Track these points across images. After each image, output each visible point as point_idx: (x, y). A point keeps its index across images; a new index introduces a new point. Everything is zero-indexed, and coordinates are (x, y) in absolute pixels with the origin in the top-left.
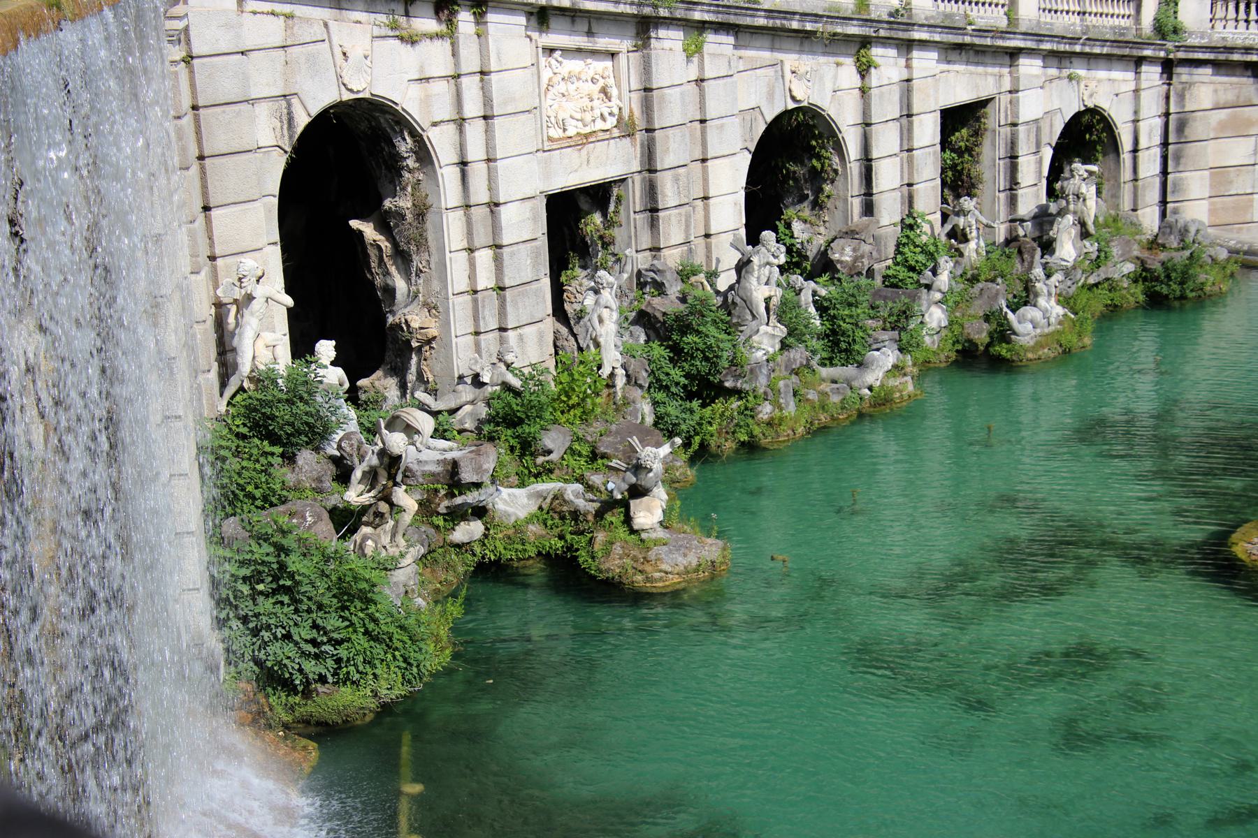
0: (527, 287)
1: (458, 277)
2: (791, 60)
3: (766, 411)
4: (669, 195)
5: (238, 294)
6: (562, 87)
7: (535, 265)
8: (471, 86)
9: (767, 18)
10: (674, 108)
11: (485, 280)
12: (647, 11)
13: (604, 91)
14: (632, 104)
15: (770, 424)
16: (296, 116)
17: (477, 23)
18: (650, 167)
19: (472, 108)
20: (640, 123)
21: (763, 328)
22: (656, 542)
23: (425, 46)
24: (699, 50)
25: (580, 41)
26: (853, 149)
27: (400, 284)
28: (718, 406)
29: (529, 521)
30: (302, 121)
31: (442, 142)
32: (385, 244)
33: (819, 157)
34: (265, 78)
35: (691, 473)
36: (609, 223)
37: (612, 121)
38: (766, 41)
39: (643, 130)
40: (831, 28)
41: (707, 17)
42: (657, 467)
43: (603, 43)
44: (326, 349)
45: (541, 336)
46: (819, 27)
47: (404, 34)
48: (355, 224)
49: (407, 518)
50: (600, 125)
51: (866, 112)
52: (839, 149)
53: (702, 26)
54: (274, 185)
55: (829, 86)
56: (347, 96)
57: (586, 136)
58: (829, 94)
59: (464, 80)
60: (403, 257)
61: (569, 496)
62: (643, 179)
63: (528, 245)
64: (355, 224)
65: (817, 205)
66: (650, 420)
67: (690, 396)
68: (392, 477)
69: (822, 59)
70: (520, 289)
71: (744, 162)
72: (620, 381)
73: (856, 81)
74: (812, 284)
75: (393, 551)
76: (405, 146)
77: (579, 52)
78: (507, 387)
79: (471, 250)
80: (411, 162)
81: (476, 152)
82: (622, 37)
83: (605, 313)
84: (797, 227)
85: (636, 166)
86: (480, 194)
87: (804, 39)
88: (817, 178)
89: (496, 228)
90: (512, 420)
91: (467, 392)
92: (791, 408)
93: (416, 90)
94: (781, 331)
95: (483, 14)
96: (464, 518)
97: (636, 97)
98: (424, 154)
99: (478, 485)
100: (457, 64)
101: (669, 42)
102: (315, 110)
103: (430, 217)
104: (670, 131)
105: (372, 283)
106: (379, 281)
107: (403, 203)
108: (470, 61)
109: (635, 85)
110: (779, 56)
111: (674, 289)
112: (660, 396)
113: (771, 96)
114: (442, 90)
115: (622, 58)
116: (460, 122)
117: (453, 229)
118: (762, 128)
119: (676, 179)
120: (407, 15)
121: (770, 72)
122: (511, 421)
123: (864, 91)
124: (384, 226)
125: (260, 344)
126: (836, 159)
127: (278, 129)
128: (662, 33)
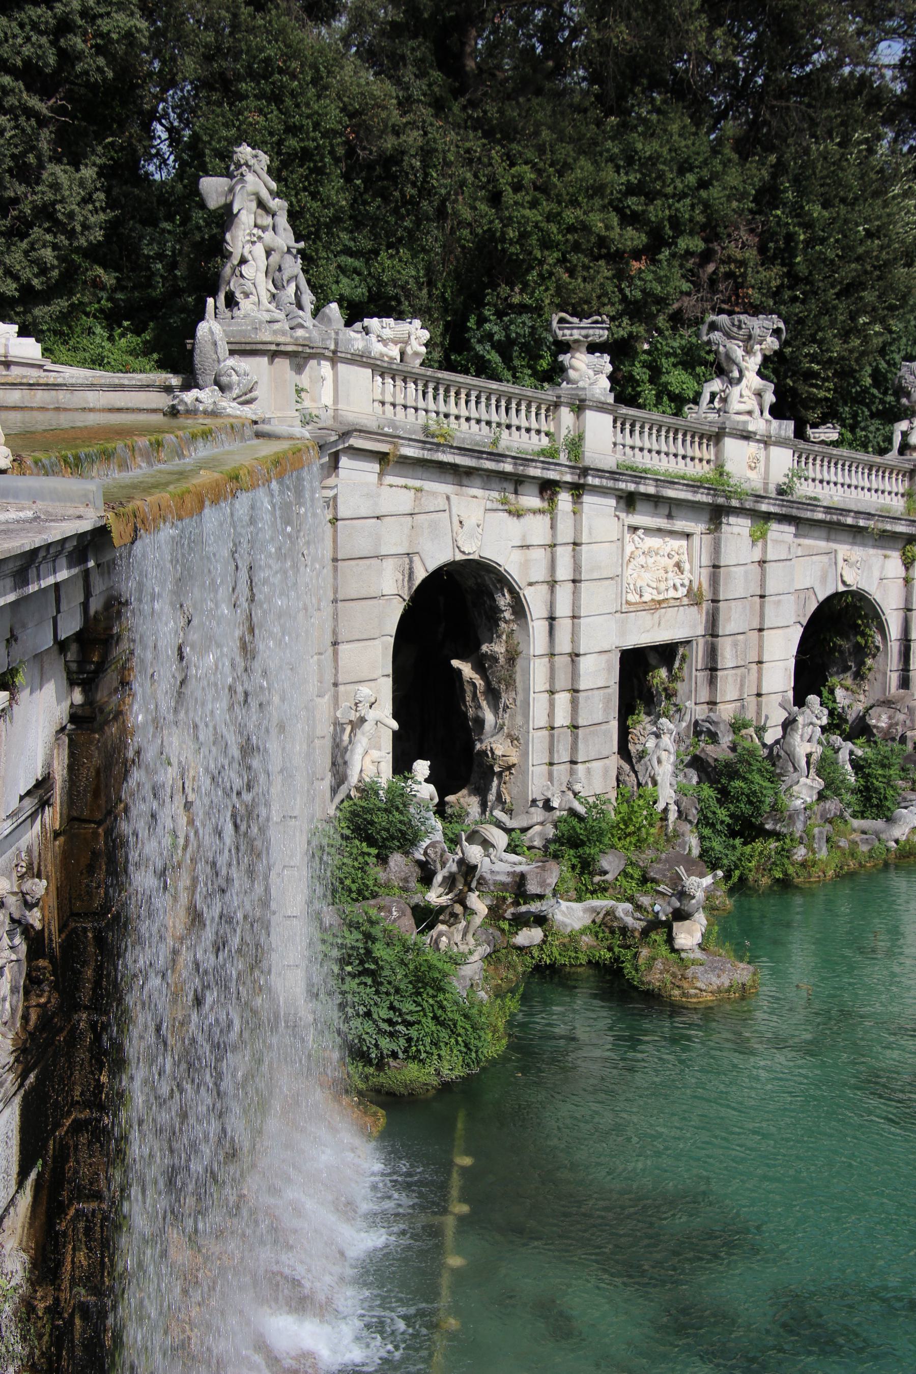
1: (538, 714)
2: (843, 550)
3: (800, 853)
4: (727, 657)
5: (353, 716)
6: (642, 560)
7: (606, 709)
8: (564, 555)
10: (738, 584)
11: (562, 718)
12: (721, 501)
13: (678, 565)
14: (702, 578)
15: (804, 865)
17: (574, 503)
19: (564, 572)
20: (707, 594)
21: (803, 780)
22: (694, 962)
23: (529, 519)
24: (763, 536)
25: (660, 522)
26: (894, 631)
27: (489, 717)
28: (758, 845)
29: (583, 932)
30: (420, 575)
31: (535, 600)
32: (479, 683)
33: (863, 635)
34: (394, 539)
35: (729, 903)
36: (673, 678)
37: (682, 591)
38: (823, 533)
39: (709, 600)
40: (881, 526)
41: (772, 509)
42: (700, 895)
43: (680, 525)
44: (422, 768)
45: (606, 771)
46: (871, 524)
47: (512, 508)
48: (455, 663)
49: (478, 920)
50: (672, 594)
51: (908, 599)
52: (882, 629)
53: (768, 517)
54: (392, 625)
55: (876, 574)
56: (459, 557)
57: (660, 602)
58: (876, 582)
59: (559, 549)
60: (493, 695)
61: (620, 913)
62: (706, 643)
63: (602, 692)
64: (455, 663)
65: (859, 676)
66: (696, 852)
67: (733, 834)
68: (468, 884)
69: (872, 551)
71: (798, 632)
72: (672, 816)
73: (901, 572)
74: (849, 745)
75: (464, 948)
76: (503, 601)
77: (659, 531)
78: (572, 812)
79: (552, 692)
80: (507, 615)
81: (563, 609)
82: (697, 521)
83: (664, 755)
84: (839, 693)
85: (701, 631)
86: (564, 645)
87: (857, 534)
88: (861, 652)
89: (575, 674)
90: (575, 842)
91: (538, 814)
92: (823, 854)
93: (517, 555)
94: (819, 784)
95: (579, 496)
96: (527, 924)
97: (705, 573)
98: (519, 609)
99: (541, 897)
100: (554, 536)
101: (738, 529)
102: (431, 569)
103: (519, 663)
104: (733, 603)
105: (465, 714)
106: (471, 712)
107: (498, 648)
108: (565, 533)
109: (705, 561)
110: (834, 546)
111: (726, 739)
112: (707, 832)
113: (824, 579)
114: (540, 556)
115: (696, 539)
116: (552, 584)
117: (537, 674)
118: (813, 606)
119: (735, 645)
120: (516, 492)
121: (825, 559)
122: (574, 842)
123: (907, 581)
124: (480, 668)
125: (368, 759)
126: (878, 638)
128: (732, 520)
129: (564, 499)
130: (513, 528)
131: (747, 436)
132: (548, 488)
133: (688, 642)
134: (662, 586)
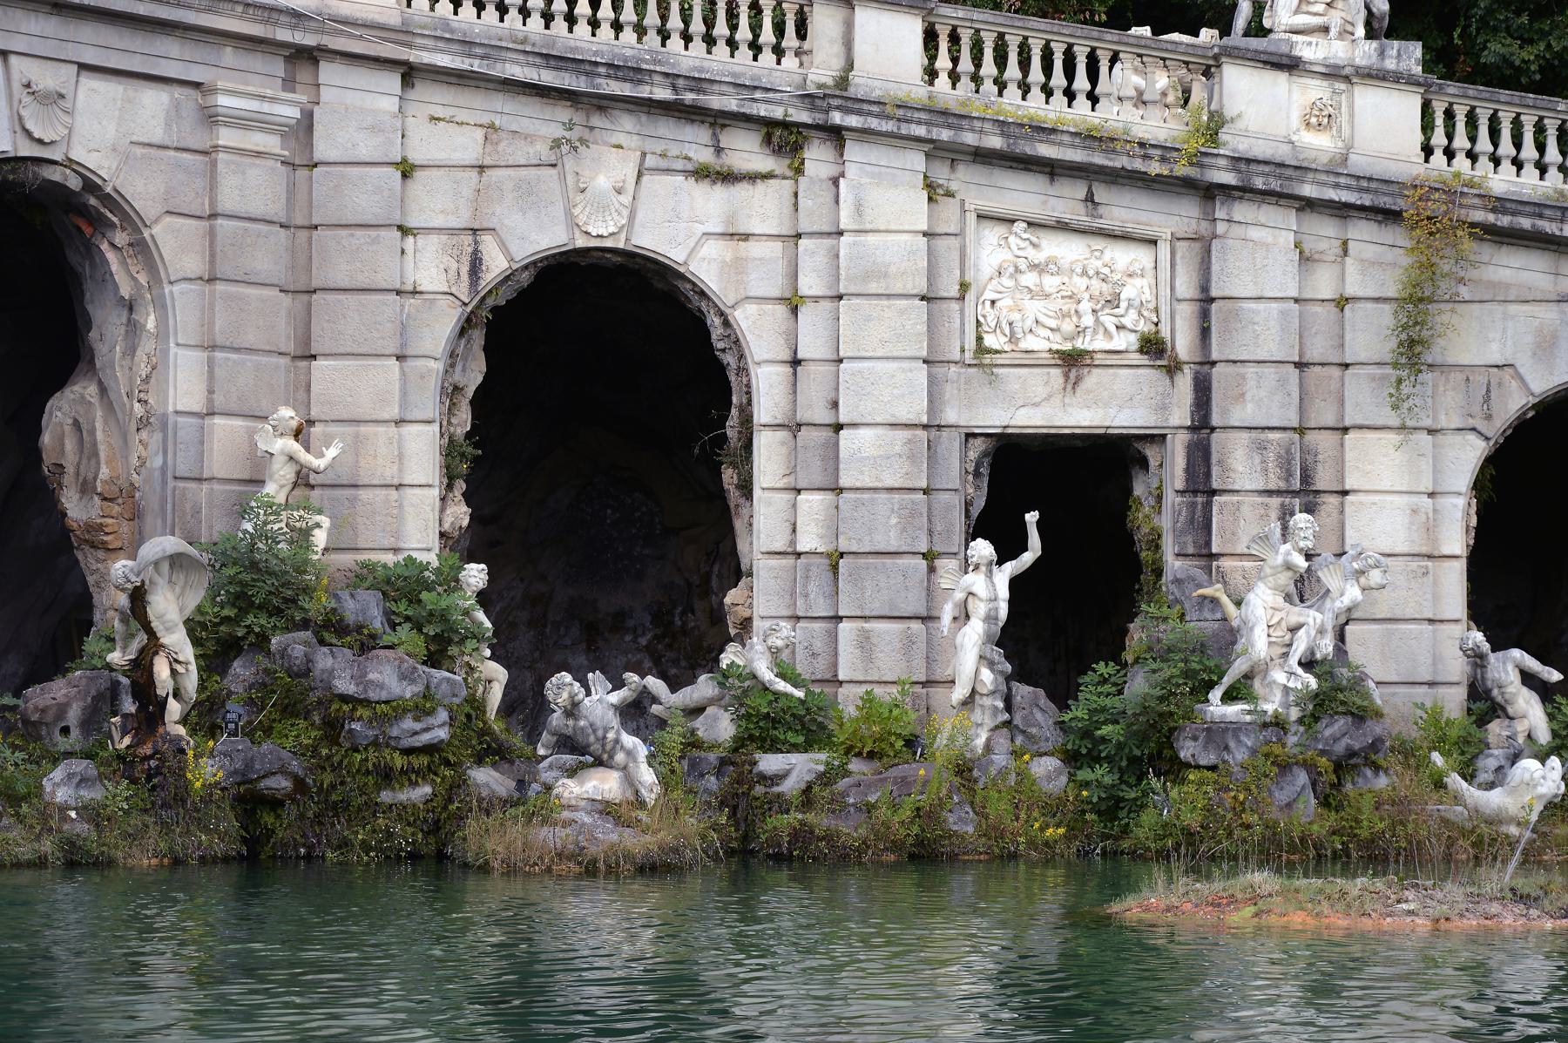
0: (888, 561)
9: (1485, 208)
10: (1260, 334)
16: (486, 257)
18: (1202, 424)
30: (496, 265)
56: (581, 242)
63: (897, 496)
70: (871, 560)
77: (1062, 227)
85: (1181, 414)
93: (713, 249)
104: (1251, 370)
115: (1164, 250)
118: (1513, 404)
127: (452, 273)
129: (817, 158)
130: (712, 202)
131: (1290, 65)
132: (785, 139)
133: (1164, 436)
134: (1068, 326)
